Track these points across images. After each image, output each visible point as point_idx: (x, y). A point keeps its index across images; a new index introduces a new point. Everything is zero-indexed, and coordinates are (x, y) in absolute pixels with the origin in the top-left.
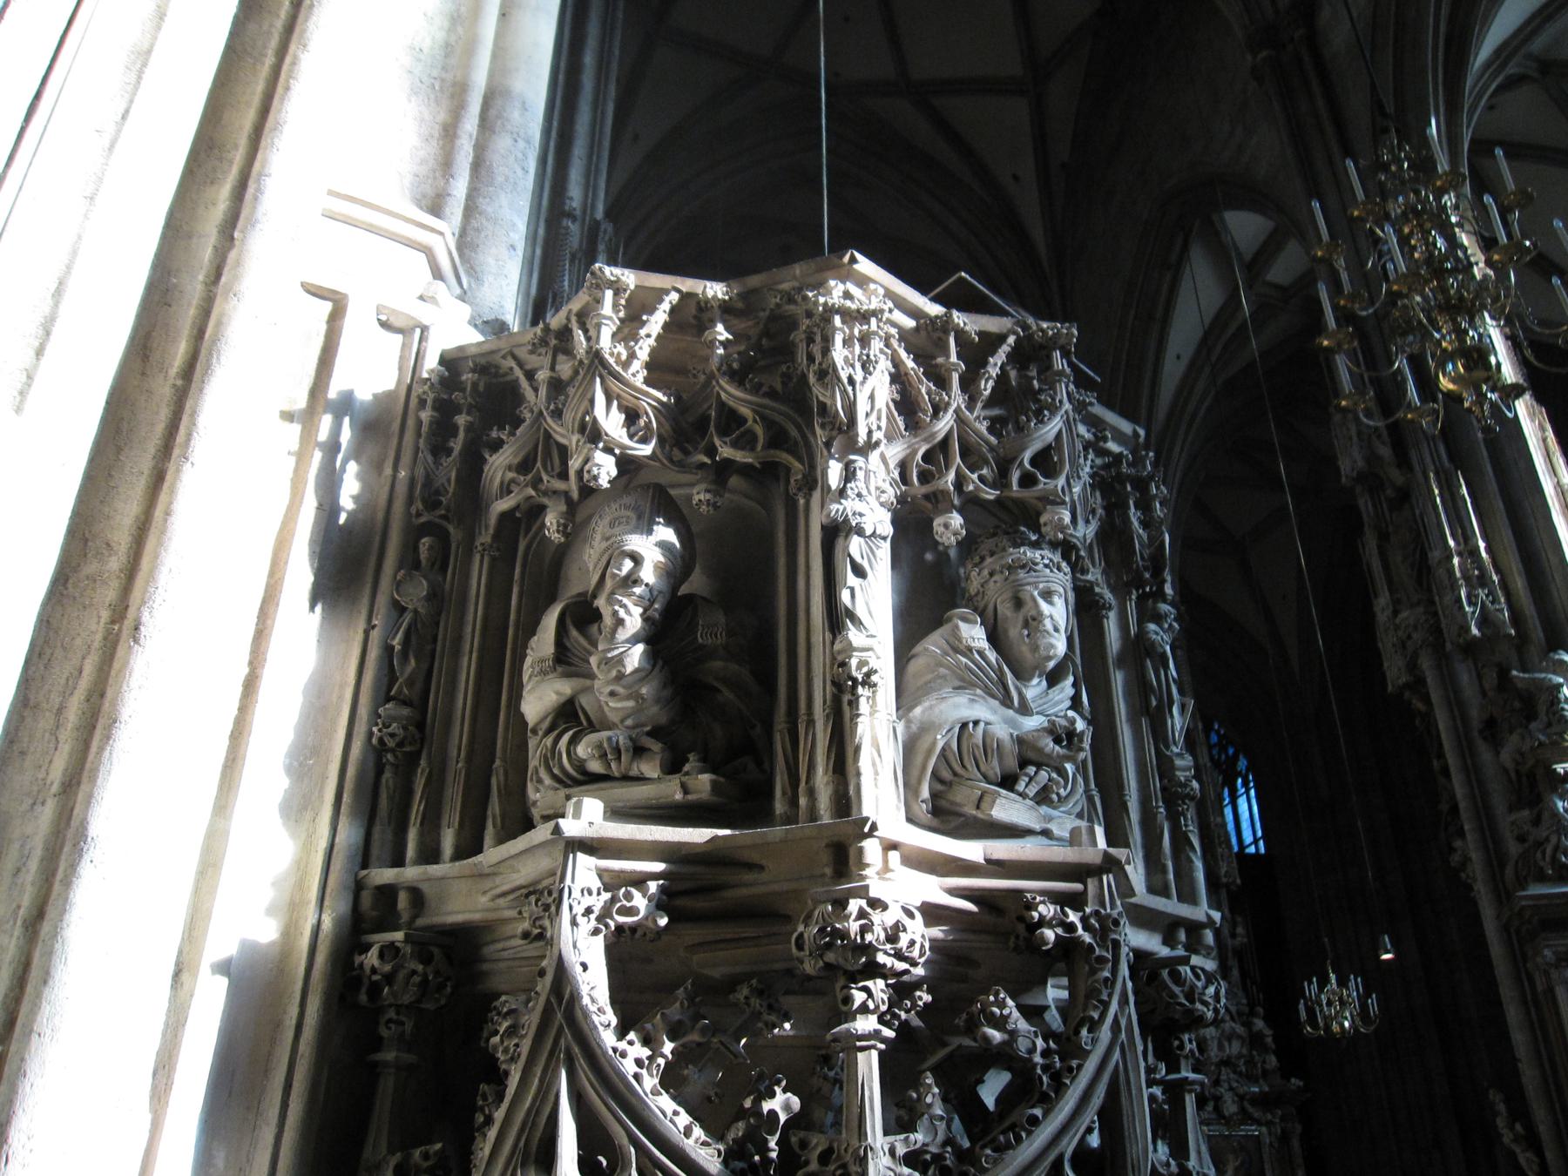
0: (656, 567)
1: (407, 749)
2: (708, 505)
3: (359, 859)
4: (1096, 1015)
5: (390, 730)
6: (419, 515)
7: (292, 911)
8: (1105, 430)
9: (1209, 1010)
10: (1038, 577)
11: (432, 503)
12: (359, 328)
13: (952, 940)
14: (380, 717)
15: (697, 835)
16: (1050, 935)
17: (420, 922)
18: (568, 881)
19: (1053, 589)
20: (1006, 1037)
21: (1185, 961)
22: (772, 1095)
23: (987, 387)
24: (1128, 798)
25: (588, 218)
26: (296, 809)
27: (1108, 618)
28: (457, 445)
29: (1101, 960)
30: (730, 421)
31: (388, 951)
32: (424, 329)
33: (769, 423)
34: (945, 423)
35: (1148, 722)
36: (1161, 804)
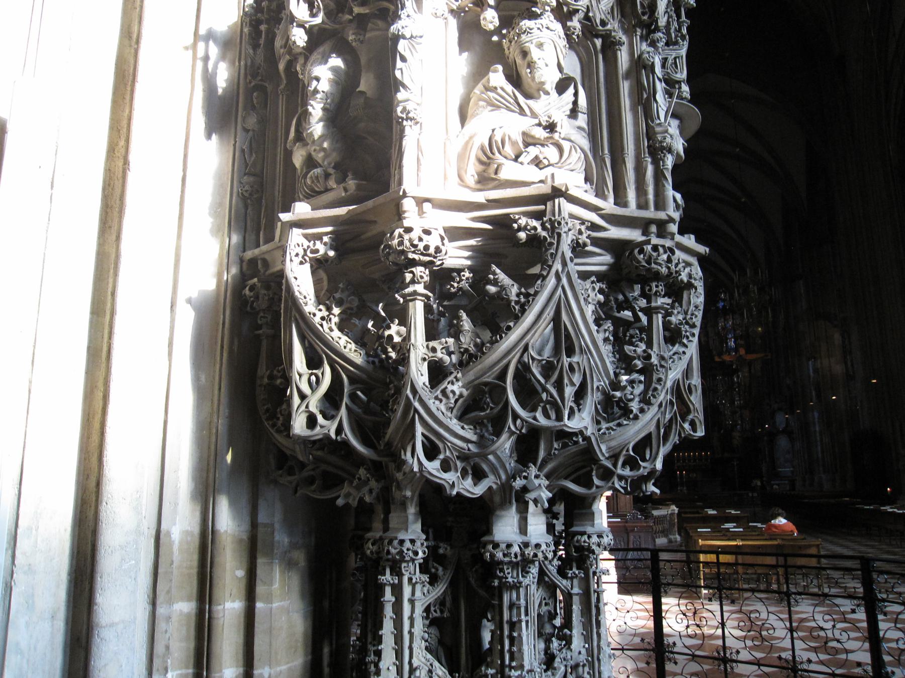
0: (330, 80)
1: (255, 196)
2: (356, 41)
3: (242, 249)
4: (545, 273)
5: (245, 189)
6: (250, 82)
7: (219, 275)
9: (662, 268)
11: (254, 76)
13: (480, 245)
14: (242, 183)
15: (342, 211)
16: (522, 235)
17: (268, 272)
18: (289, 242)
19: (542, 41)
20: (499, 289)
21: (648, 242)
22: (389, 328)
24: (627, 155)
27: (620, 50)
28: (262, 41)
29: (551, 244)
31: (252, 288)
35: (642, 109)
36: (647, 155)
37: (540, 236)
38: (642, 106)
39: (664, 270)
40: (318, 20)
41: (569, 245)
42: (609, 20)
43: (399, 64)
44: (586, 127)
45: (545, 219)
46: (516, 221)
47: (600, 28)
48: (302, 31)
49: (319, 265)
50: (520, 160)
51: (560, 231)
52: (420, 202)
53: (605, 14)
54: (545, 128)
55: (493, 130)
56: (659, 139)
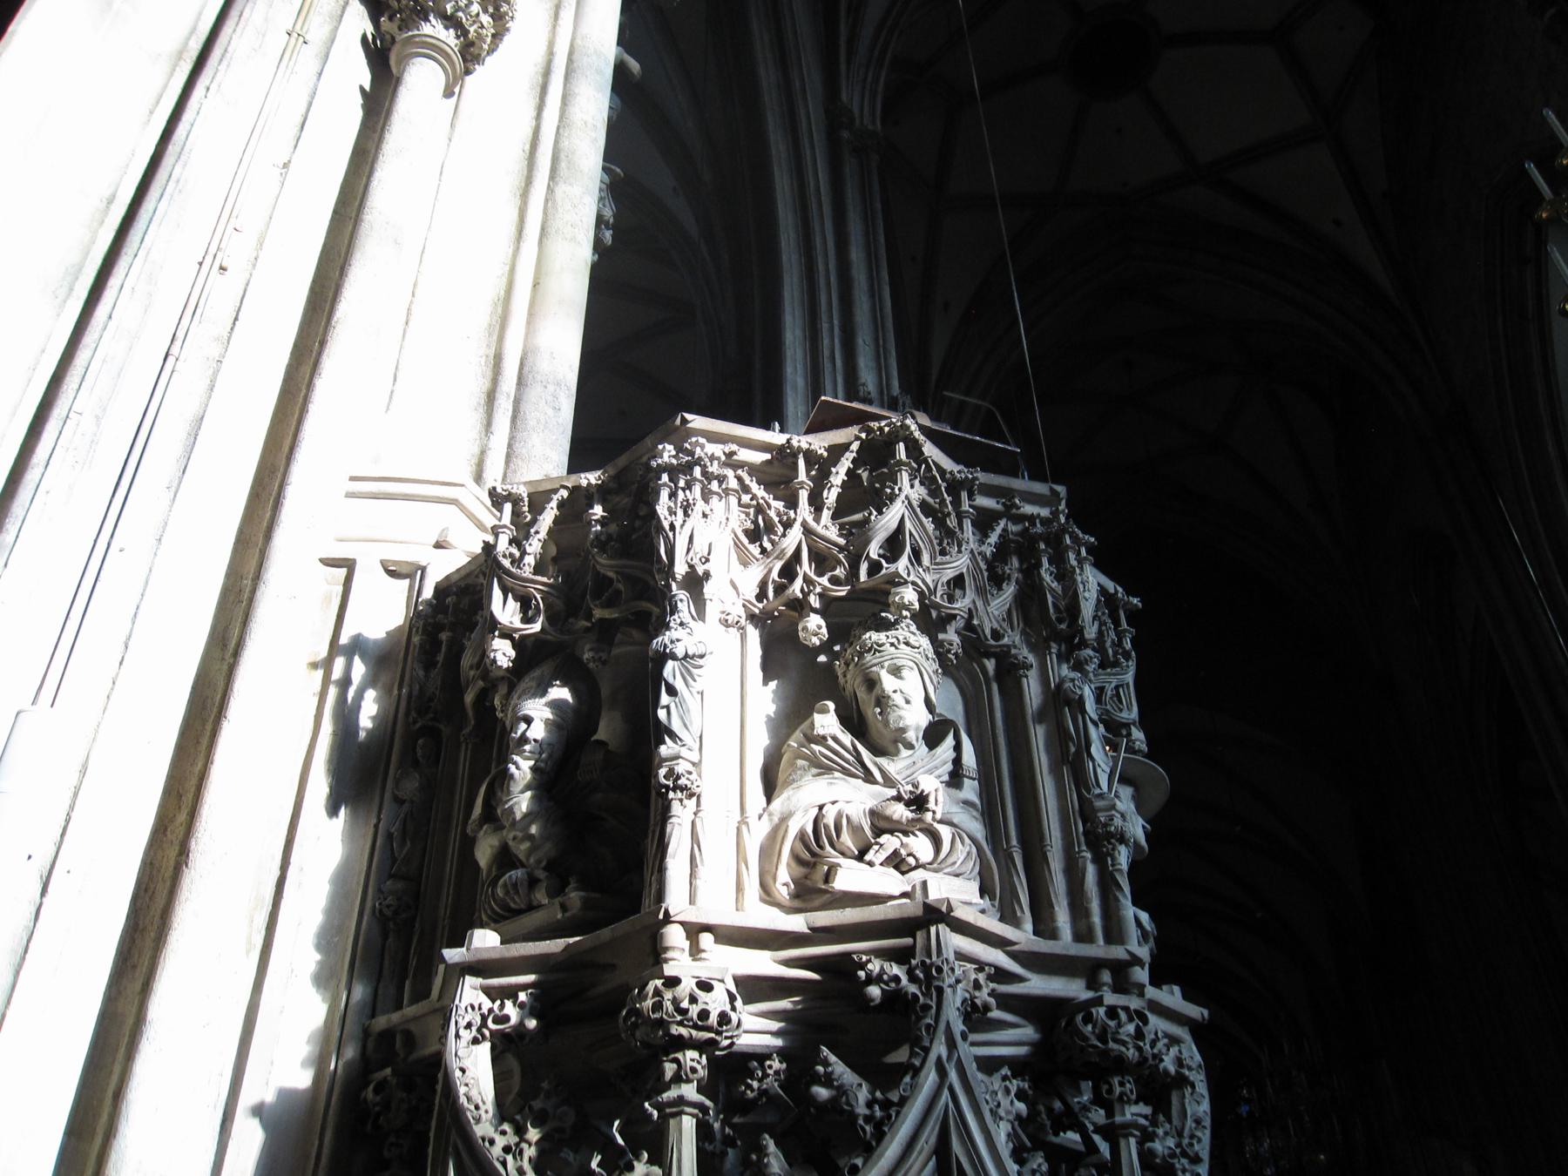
0: (547, 722)
2: (594, 662)
4: (917, 1063)
5: (387, 902)
7: (320, 1062)
8: (1013, 497)
9: (1128, 1049)
10: (882, 657)
12: (369, 578)
13: (801, 1010)
14: (382, 892)
16: (875, 991)
18: (457, 1002)
20: (834, 1092)
21: (1098, 1001)
23: (831, 496)
24: (1049, 848)
25: (886, 398)
26: (323, 979)
27: (1027, 677)
28: (440, 658)
29: (926, 1008)
30: (602, 583)
32: (423, 569)
33: (627, 578)
34: (795, 536)
35: (1069, 769)
36: (1084, 848)
37: (906, 993)
38: (1069, 765)
39: (1131, 1053)
40: (536, 627)
41: (958, 1009)
42: (1004, 630)
43: (665, 699)
44: (976, 800)
45: (914, 962)
46: (862, 966)
47: (992, 642)
48: (508, 642)
49: (506, 1046)
50: (867, 858)
51: (941, 984)
52: (694, 931)
53: (998, 622)
54: (908, 804)
55: (821, 807)
56: (1102, 819)
